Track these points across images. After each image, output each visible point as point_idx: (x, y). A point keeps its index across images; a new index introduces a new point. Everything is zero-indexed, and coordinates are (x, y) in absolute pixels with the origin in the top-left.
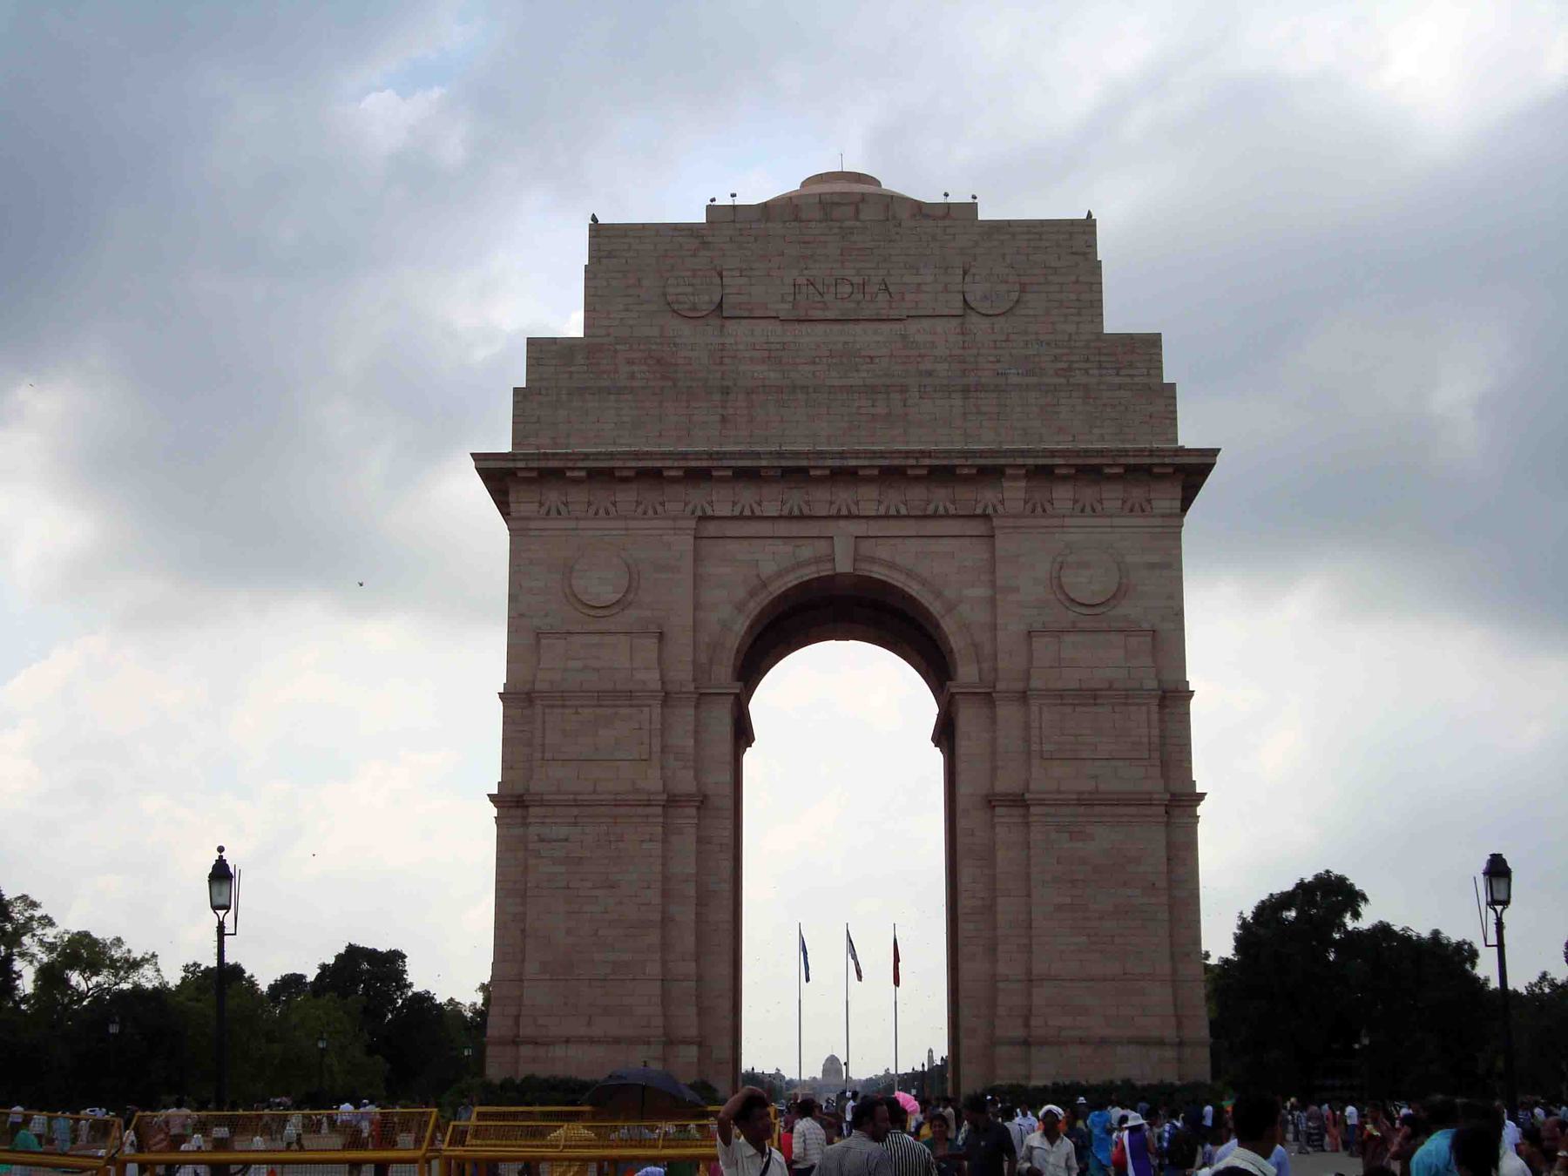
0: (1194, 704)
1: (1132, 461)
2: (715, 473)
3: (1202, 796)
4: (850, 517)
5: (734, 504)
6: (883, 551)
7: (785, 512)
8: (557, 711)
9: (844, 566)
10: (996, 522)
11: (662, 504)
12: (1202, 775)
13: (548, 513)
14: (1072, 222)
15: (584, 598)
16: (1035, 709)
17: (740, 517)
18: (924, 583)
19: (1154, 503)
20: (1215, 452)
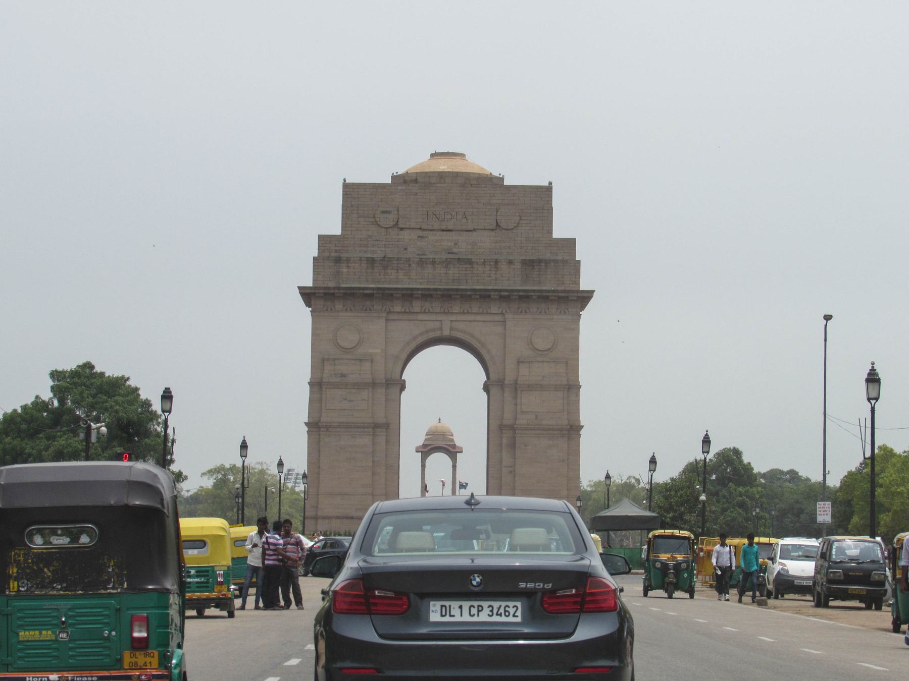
0: (582, 392)
4: (448, 313)
9: (446, 333)
12: (584, 418)
16: (519, 392)
17: (405, 312)
20: (593, 292)
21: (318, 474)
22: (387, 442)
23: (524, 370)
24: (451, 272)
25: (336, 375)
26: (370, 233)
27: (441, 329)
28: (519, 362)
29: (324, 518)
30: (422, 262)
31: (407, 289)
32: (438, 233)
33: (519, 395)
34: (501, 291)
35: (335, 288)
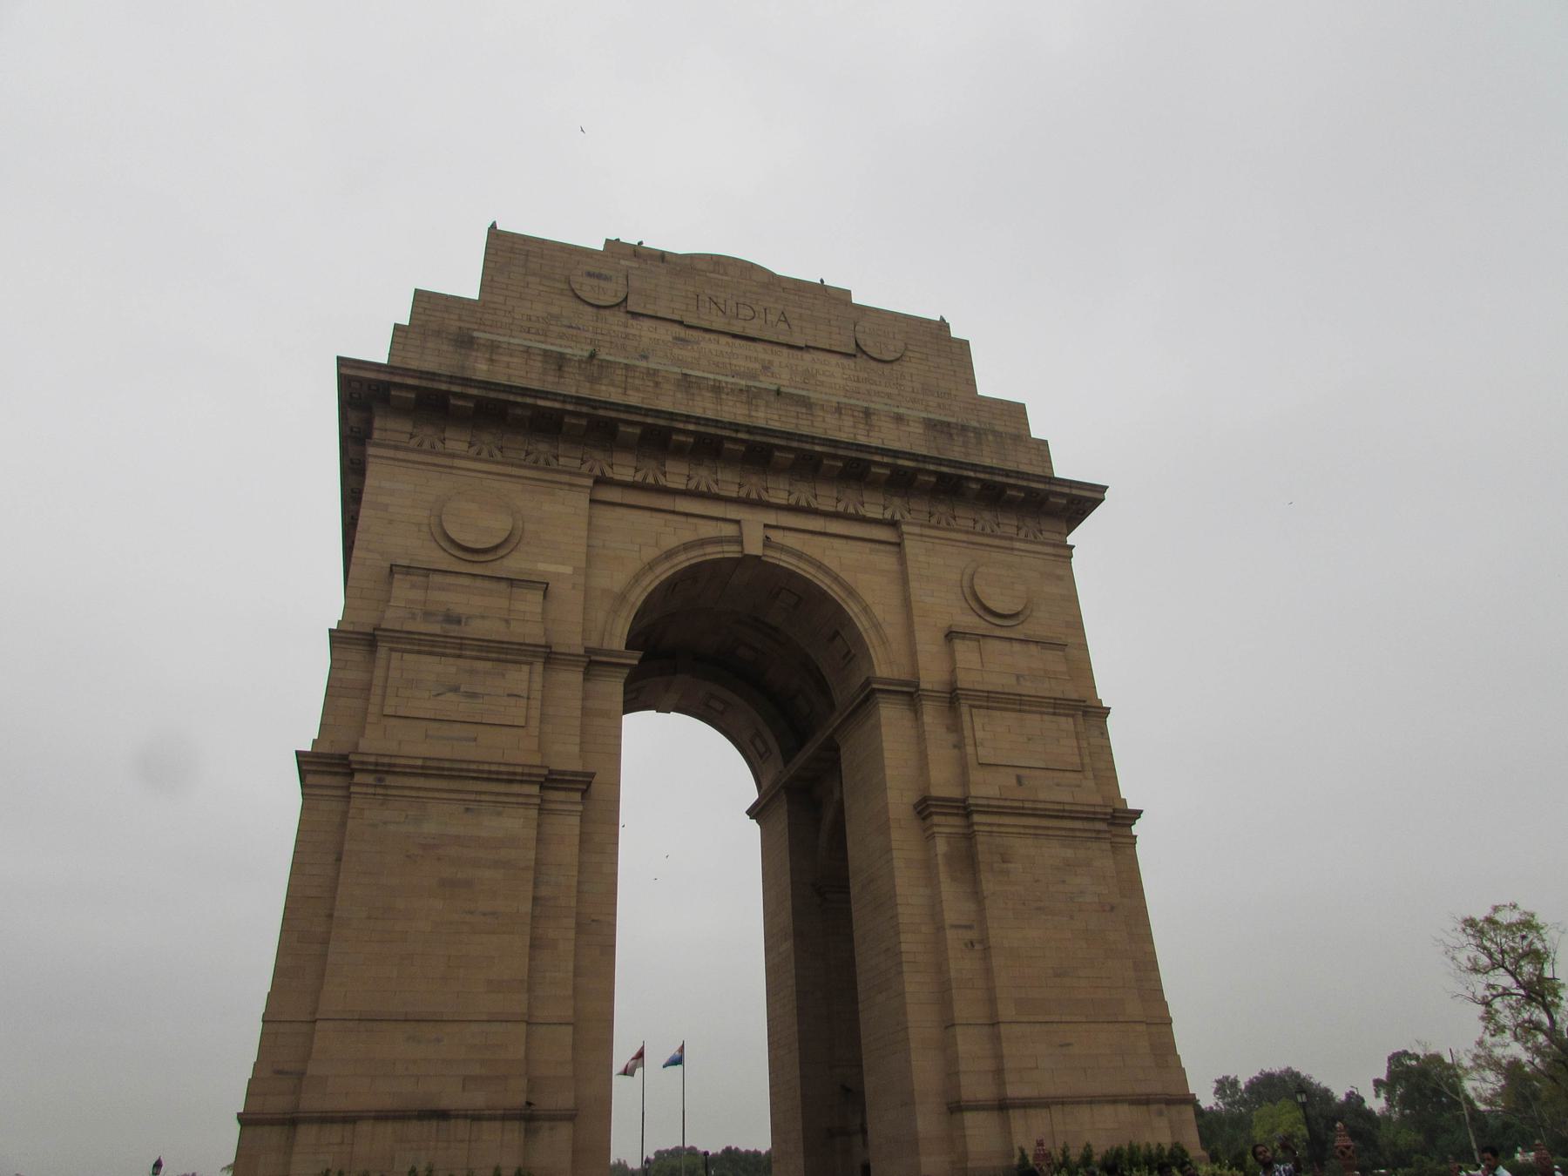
1: (1034, 485)
2: (622, 428)
3: (1137, 814)
5: (637, 470)
6: (790, 540)
7: (692, 485)
8: (406, 656)
9: (754, 547)
10: (905, 528)
11: (556, 457)
13: (420, 445)
14: (929, 321)
15: (453, 536)
16: (965, 710)
18: (836, 578)
19: (1046, 534)
21: (326, 942)
22: (584, 840)
23: (966, 653)
24: (761, 414)
25: (427, 615)
26: (555, 310)
27: (739, 540)
28: (951, 635)
29: (325, 1119)
30: (687, 383)
31: (658, 413)
32: (724, 340)
33: (966, 718)
34: (896, 454)
35: (452, 379)
